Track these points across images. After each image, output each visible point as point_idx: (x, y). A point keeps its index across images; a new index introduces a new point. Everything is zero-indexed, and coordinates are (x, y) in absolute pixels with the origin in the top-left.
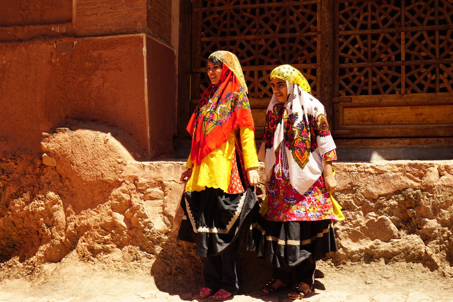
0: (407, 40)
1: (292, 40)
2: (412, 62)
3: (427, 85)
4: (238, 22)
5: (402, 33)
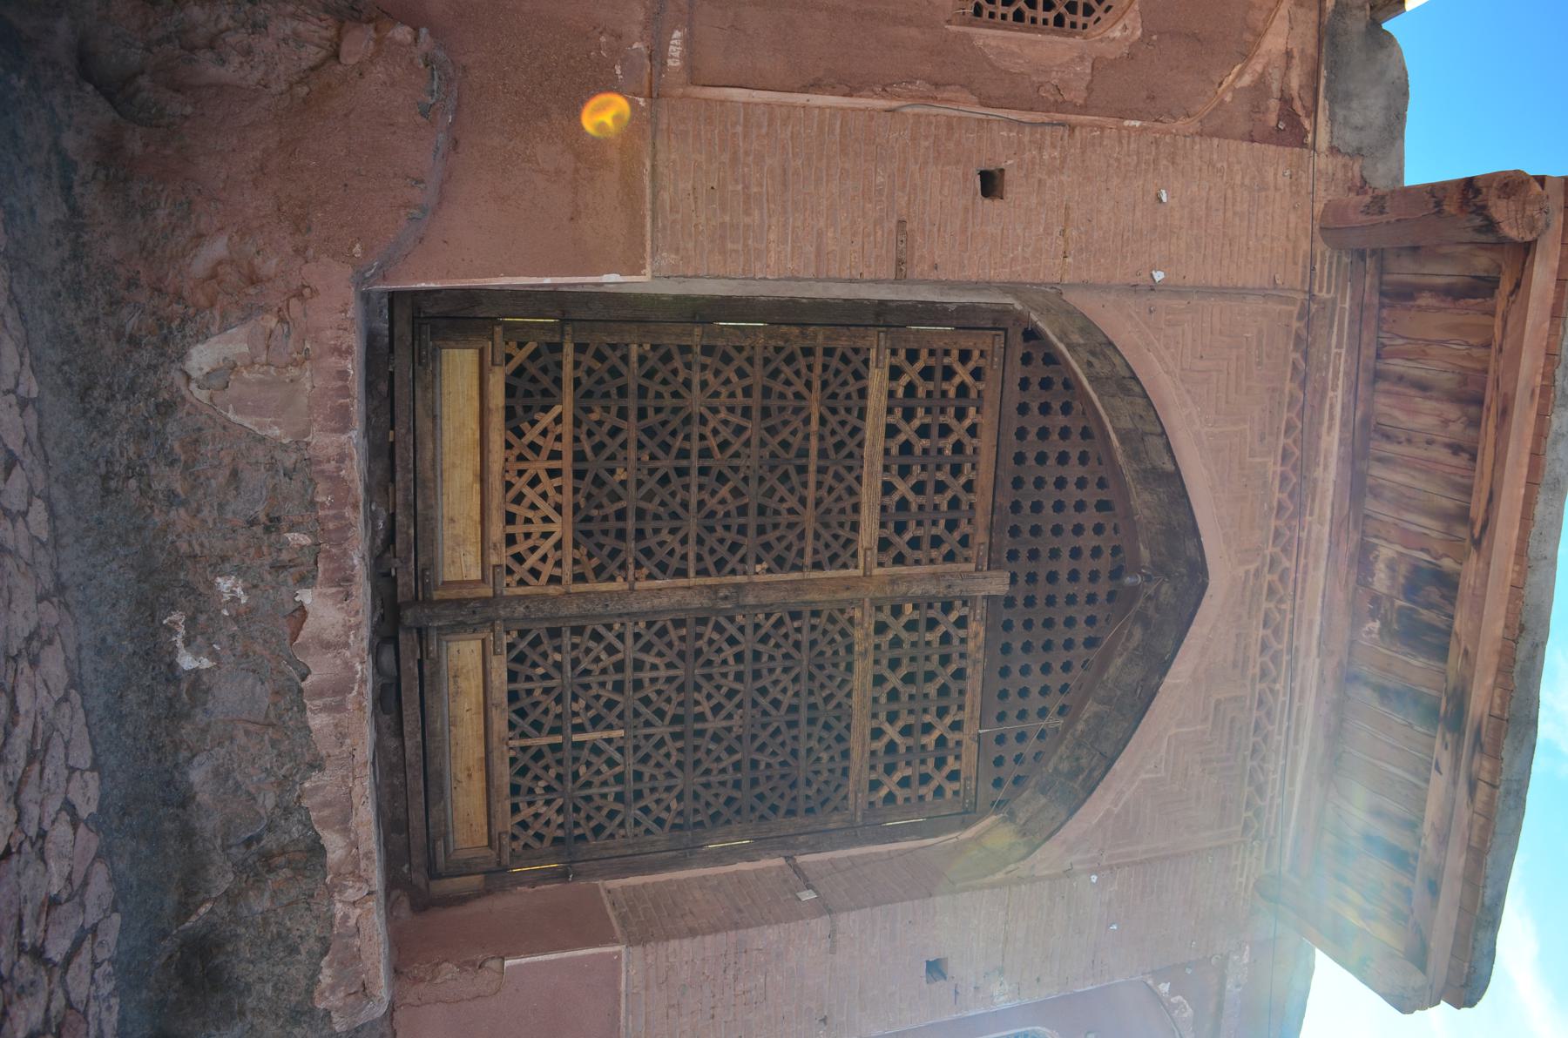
0: (609, 741)
1: (621, 535)
2: (568, 753)
3: (525, 782)
4: (664, 423)
5: (621, 733)
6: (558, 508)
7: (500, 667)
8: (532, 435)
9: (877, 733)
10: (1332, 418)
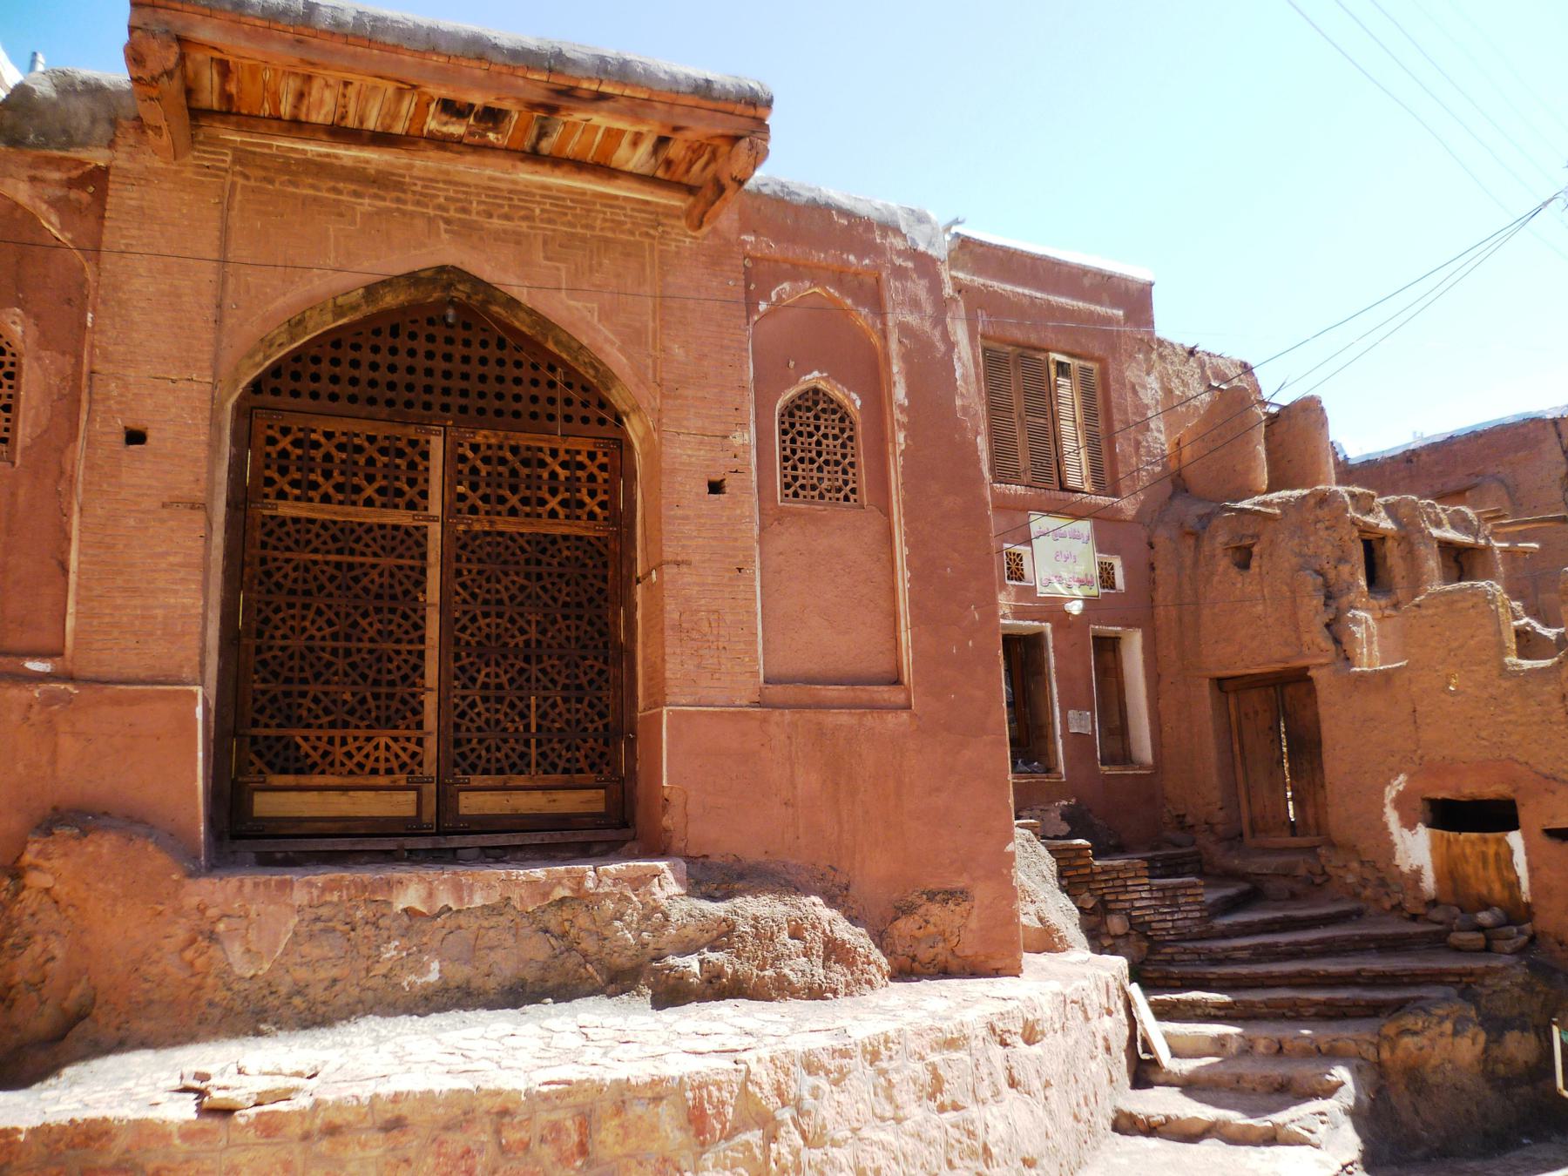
0: (538, 706)
1: (390, 696)
2: (544, 736)
3: (562, 764)
4: (312, 666)
6: (368, 739)
7: (477, 780)
8: (316, 756)
9: (553, 514)
10: (328, 155)
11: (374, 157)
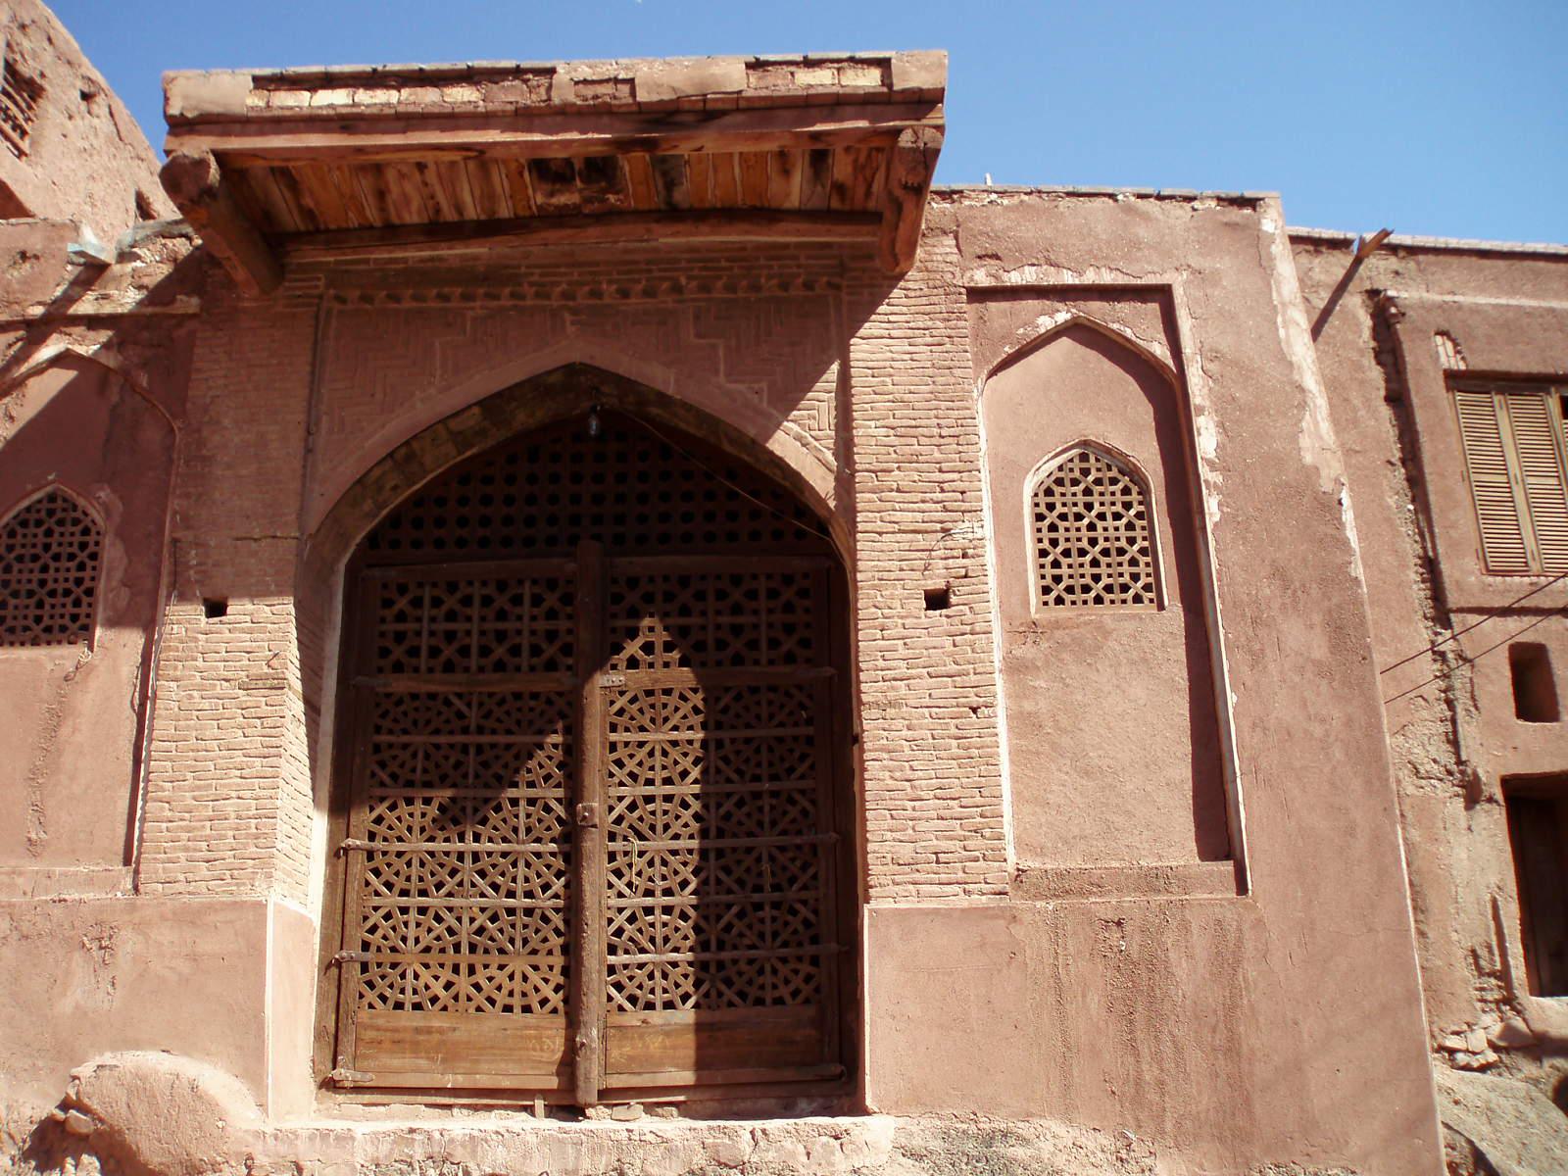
10: (432, 259)
11: (478, 250)
